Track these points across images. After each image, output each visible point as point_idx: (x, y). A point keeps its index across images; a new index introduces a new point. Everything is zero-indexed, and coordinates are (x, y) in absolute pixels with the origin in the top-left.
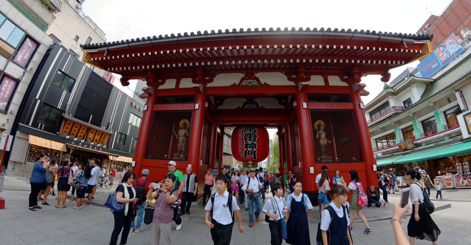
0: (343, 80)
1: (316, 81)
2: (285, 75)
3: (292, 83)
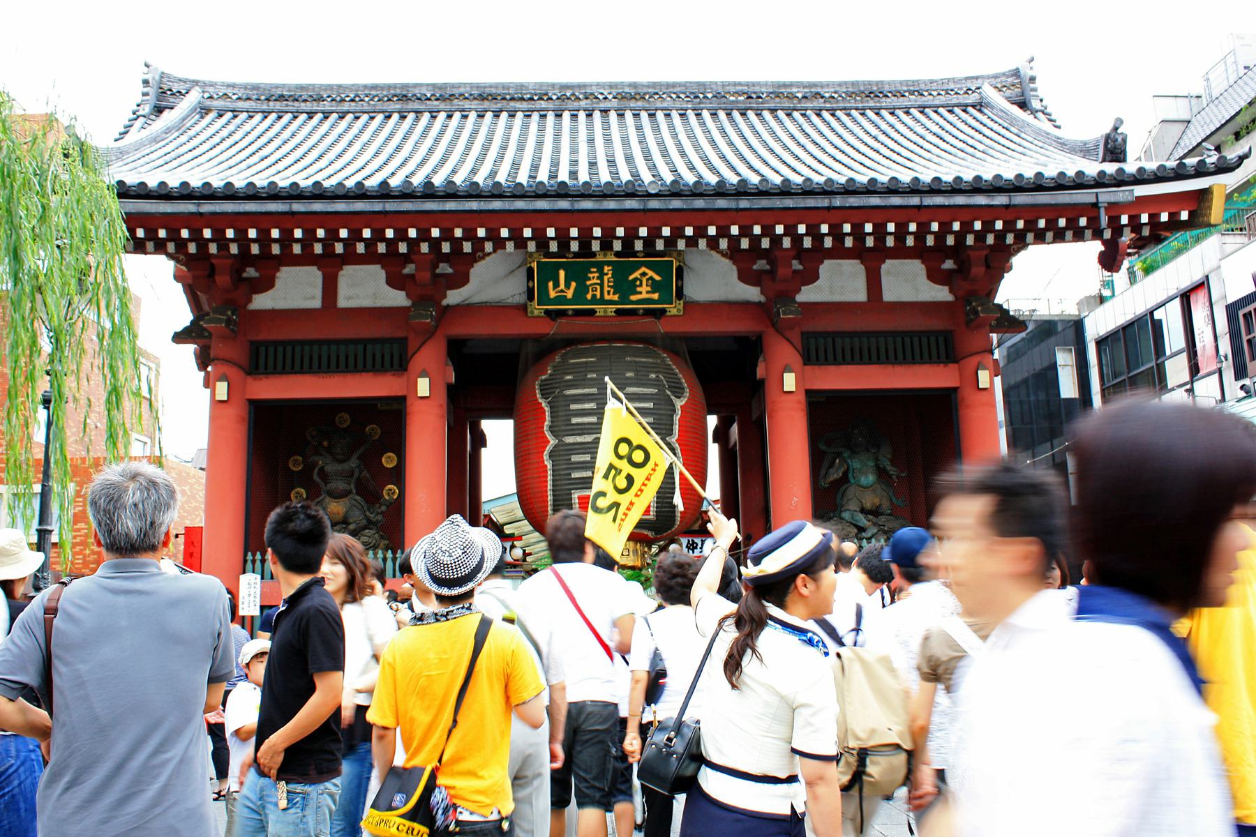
0: (935, 276)
1: (840, 282)
2: (731, 258)
3: (752, 293)
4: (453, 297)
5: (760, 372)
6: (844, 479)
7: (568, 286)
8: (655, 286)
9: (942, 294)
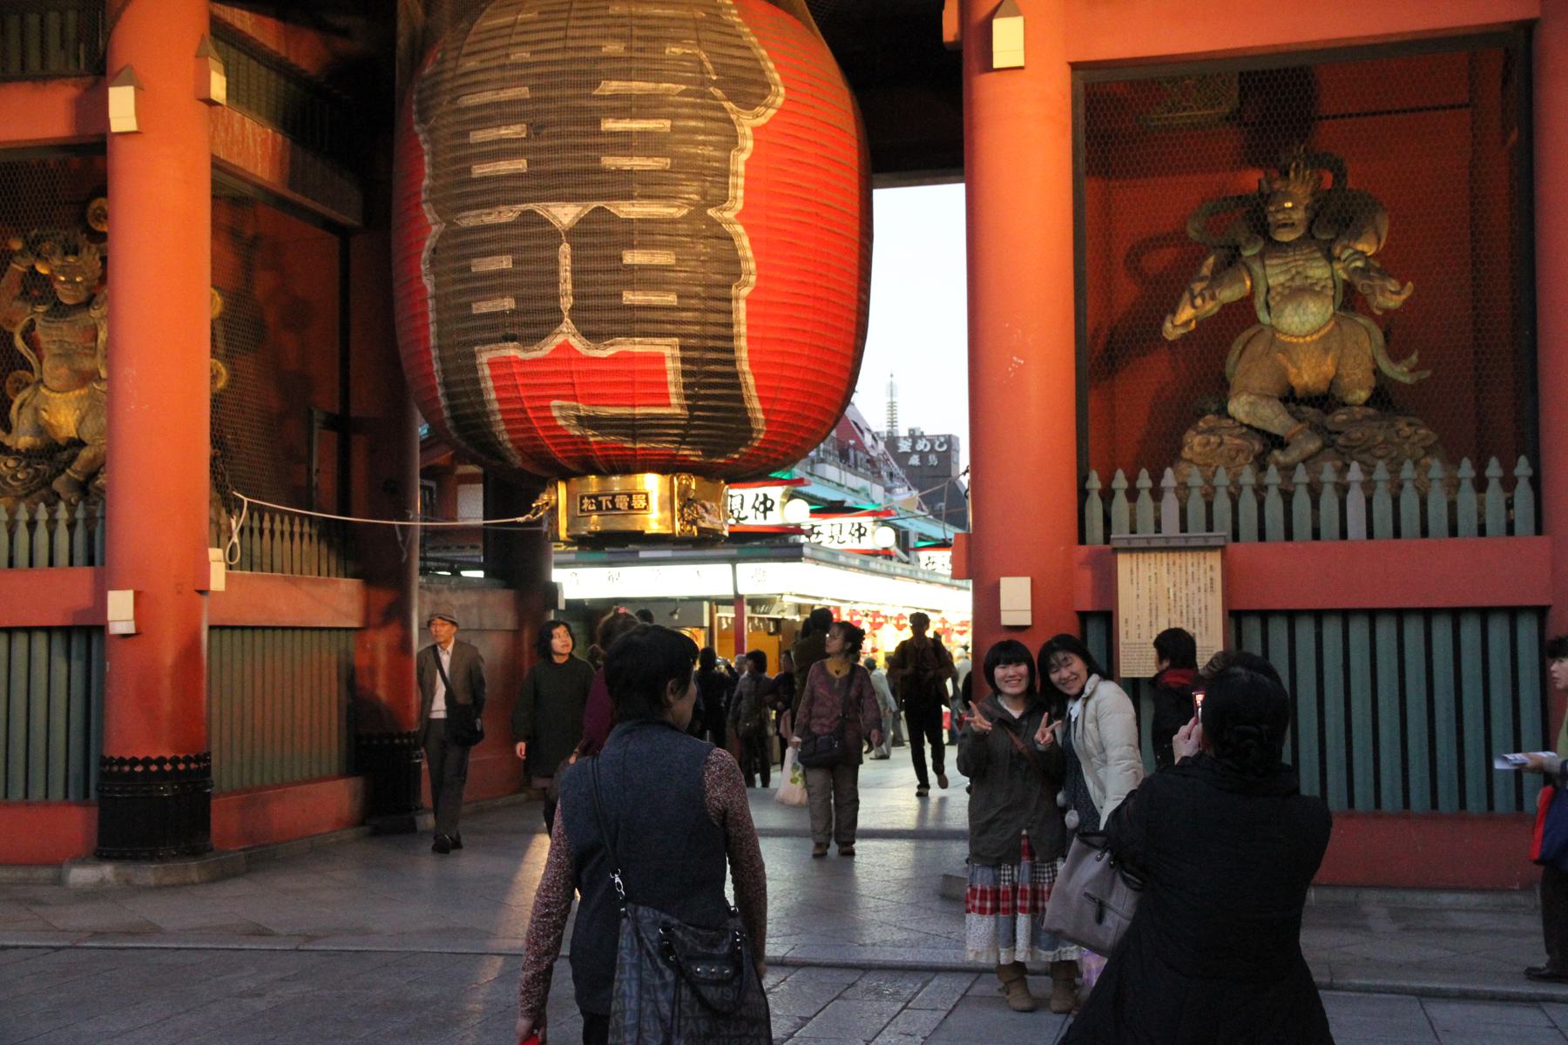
6: (1240, 316)
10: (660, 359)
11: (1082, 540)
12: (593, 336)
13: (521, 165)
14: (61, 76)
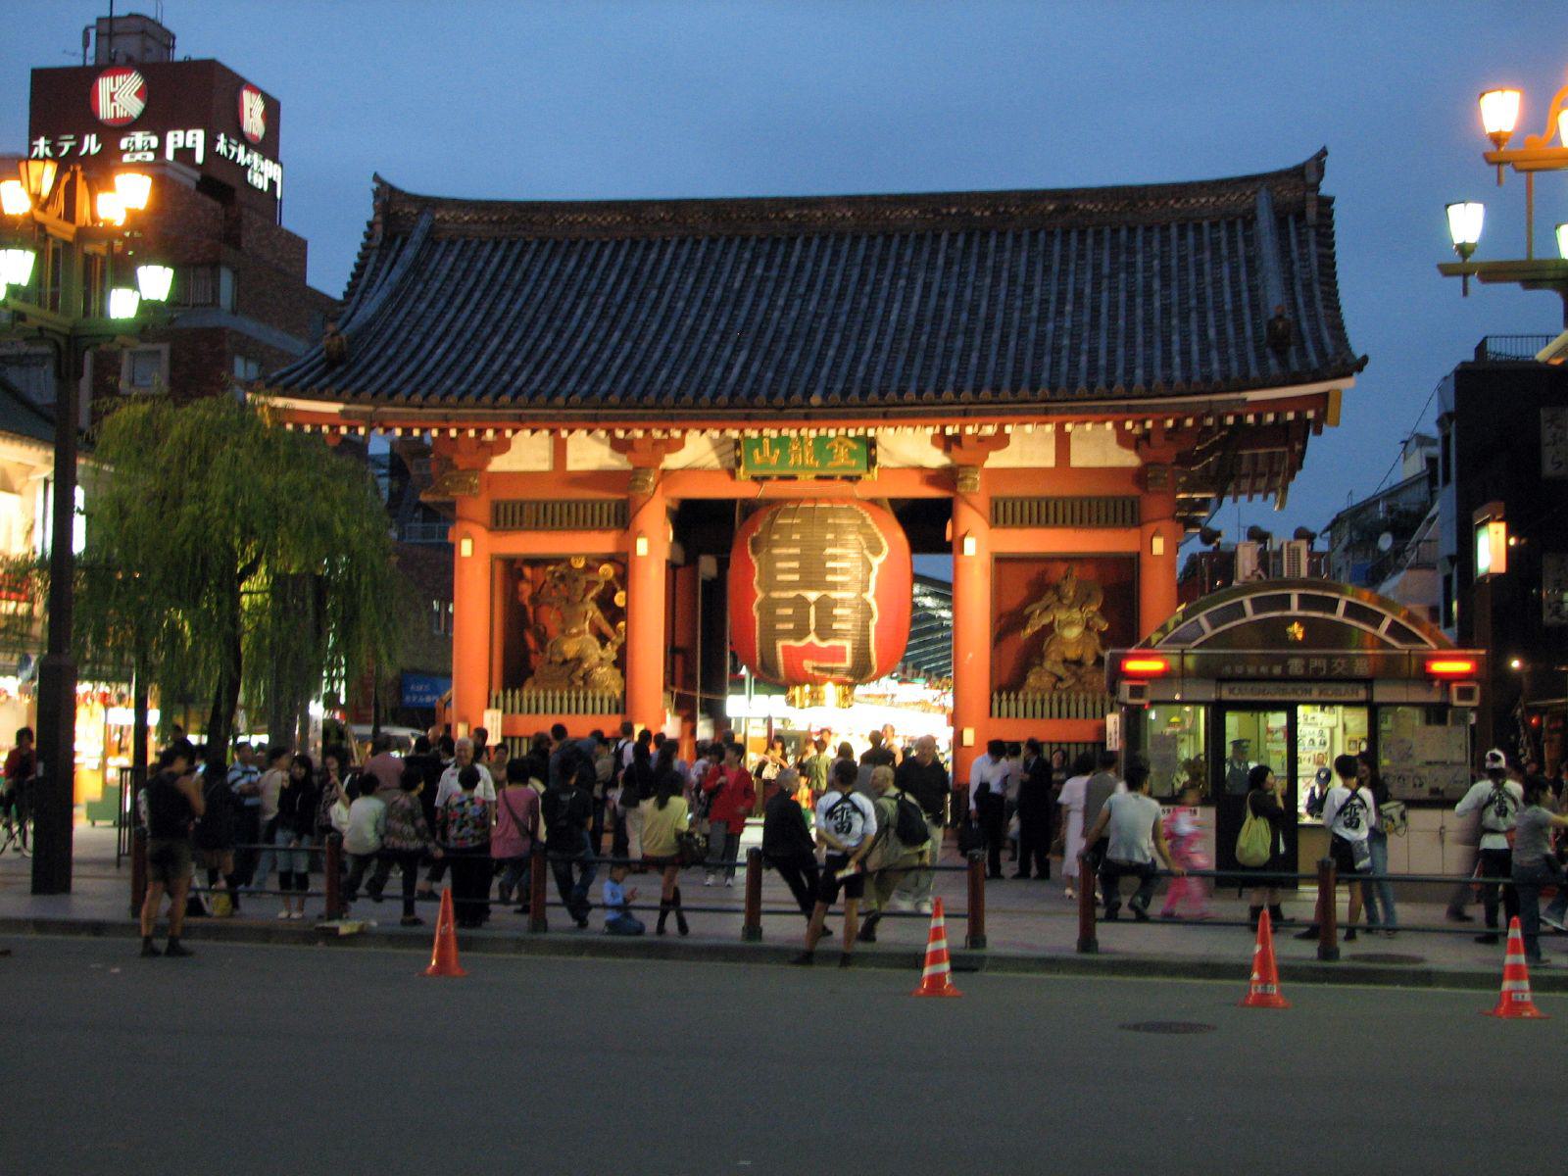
4: (673, 461)
5: (949, 535)
6: (1048, 630)
7: (772, 453)
8: (851, 454)
9: (1130, 459)
10: (844, 648)
11: (991, 714)
12: (823, 639)
13: (796, 577)
14: (610, 530)
